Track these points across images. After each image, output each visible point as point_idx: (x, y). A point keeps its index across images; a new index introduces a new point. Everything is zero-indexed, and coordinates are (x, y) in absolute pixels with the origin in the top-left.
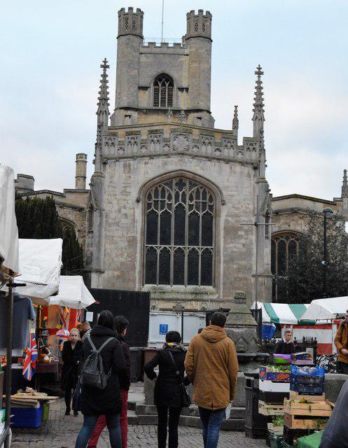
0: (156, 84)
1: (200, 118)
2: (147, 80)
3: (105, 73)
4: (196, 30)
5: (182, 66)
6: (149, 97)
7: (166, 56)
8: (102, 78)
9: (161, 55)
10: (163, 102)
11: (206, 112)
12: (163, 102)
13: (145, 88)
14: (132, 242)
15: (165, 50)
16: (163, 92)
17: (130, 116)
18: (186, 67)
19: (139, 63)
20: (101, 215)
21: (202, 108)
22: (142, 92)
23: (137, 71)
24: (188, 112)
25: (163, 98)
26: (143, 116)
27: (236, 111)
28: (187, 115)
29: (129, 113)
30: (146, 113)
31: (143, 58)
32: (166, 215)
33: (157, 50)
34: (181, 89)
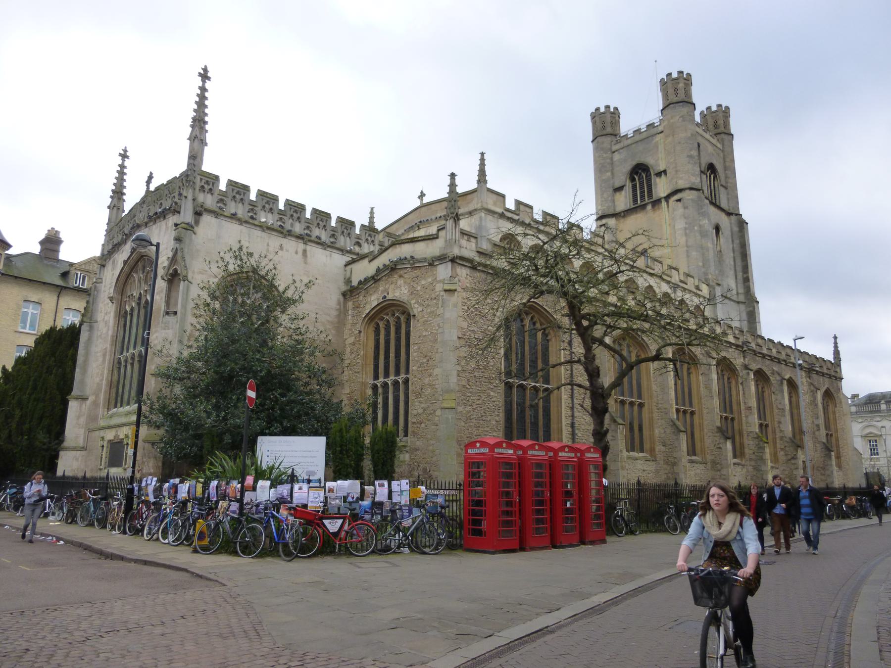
0: (633, 180)
1: (679, 200)
2: (621, 178)
3: (123, 163)
4: (676, 94)
5: (658, 147)
6: (626, 197)
7: (640, 143)
8: (119, 169)
9: (633, 146)
10: (642, 197)
11: (688, 191)
12: (642, 197)
13: (620, 189)
14: (104, 355)
15: (638, 138)
16: (642, 187)
17: (604, 225)
18: (661, 147)
19: (612, 163)
20: (91, 328)
21: (680, 187)
22: (618, 194)
23: (609, 174)
24: (667, 198)
25: (642, 192)
26: (622, 220)
27: (482, 160)
28: (667, 202)
29: (604, 221)
30: (624, 217)
31: (616, 157)
32: (132, 309)
33: (629, 142)
34: (659, 174)
